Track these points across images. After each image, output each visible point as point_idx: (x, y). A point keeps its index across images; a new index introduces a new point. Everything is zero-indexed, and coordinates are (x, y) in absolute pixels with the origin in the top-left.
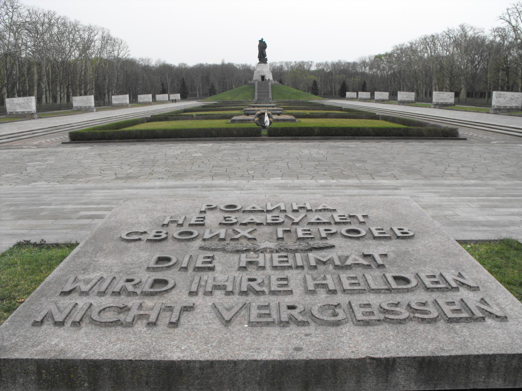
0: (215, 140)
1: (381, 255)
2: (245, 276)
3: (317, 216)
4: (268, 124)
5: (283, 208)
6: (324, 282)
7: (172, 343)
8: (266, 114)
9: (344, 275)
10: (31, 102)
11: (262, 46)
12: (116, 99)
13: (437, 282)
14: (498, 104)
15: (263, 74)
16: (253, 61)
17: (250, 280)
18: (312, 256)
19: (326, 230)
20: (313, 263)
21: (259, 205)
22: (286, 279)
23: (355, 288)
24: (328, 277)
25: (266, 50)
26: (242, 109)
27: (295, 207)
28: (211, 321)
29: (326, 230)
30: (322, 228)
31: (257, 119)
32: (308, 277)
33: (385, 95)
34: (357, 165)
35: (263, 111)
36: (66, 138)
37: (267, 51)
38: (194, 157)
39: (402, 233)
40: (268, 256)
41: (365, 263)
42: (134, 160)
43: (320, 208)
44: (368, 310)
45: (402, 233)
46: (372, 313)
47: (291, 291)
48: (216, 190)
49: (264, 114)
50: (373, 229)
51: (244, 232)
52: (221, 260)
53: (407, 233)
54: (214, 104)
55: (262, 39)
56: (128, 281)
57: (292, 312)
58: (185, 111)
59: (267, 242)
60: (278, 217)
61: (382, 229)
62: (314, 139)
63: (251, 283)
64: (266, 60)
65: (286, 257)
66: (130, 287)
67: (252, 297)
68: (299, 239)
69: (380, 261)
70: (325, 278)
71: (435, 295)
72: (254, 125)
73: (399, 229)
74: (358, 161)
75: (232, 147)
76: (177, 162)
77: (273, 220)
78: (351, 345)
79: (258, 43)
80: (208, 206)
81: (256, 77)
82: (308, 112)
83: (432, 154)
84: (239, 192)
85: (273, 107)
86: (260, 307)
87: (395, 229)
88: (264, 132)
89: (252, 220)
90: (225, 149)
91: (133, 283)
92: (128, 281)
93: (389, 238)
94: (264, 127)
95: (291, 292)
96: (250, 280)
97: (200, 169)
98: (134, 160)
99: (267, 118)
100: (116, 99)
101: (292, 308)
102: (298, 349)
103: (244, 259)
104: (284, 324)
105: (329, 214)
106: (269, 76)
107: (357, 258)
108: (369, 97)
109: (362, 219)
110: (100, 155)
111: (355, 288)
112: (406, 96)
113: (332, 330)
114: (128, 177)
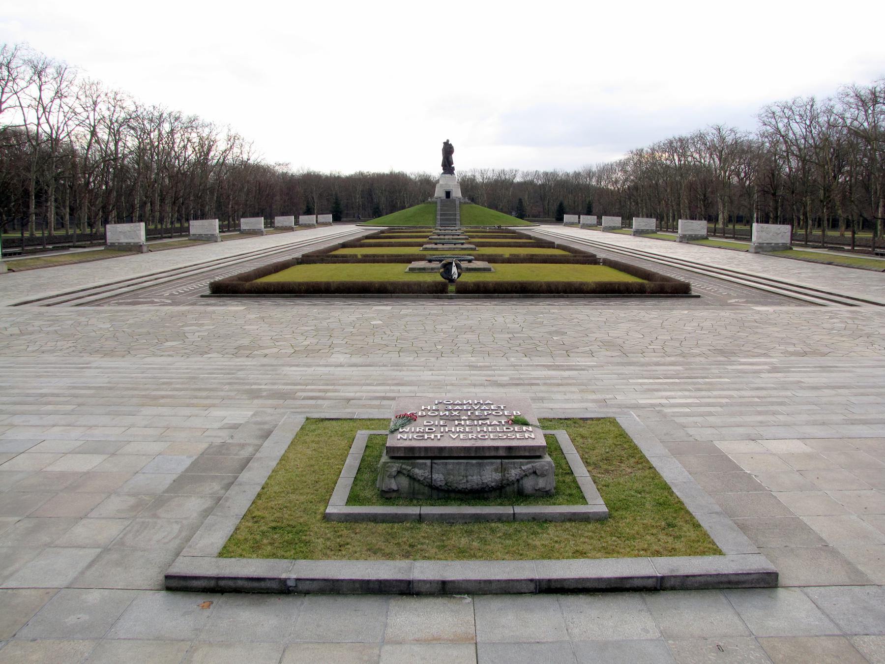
0: (392, 297)
4: (456, 276)
10: (140, 230)
11: (448, 150)
12: (246, 224)
14: (760, 241)
15: (448, 189)
16: (435, 170)
18: (480, 422)
25: (453, 156)
31: (442, 270)
33: (617, 221)
34: (555, 338)
35: (449, 260)
36: (208, 292)
37: (455, 157)
42: (306, 328)
48: (408, 370)
49: (451, 263)
51: (456, 413)
52: (448, 423)
54: (382, 232)
55: (448, 141)
58: (344, 246)
62: (512, 297)
64: (453, 169)
72: (439, 278)
74: (557, 333)
75: (415, 312)
76: (354, 331)
79: (442, 146)
81: (439, 193)
82: (507, 252)
83: (645, 322)
84: (430, 373)
85: (462, 244)
88: (452, 288)
90: (407, 315)
94: (452, 281)
97: (383, 343)
98: (306, 328)
99: (454, 270)
100: (246, 224)
103: (457, 422)
106: (457, 193)
108: (595, 222)
110: (263, 319)
114: (309, 351)
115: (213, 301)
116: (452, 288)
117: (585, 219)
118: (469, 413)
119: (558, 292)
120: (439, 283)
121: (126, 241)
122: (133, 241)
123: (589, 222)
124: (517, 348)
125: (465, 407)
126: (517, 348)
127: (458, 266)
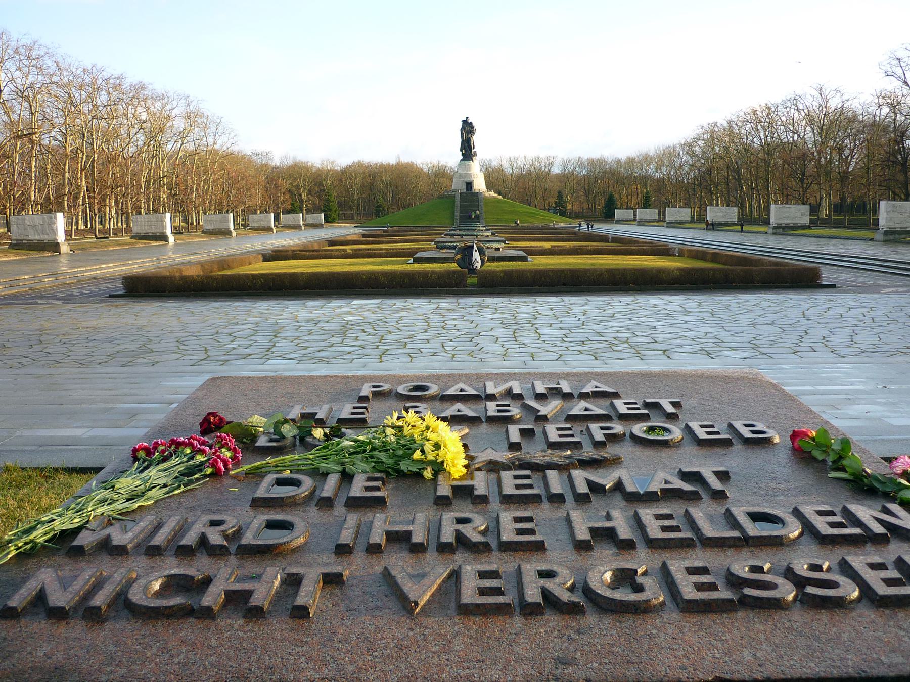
1: (717, 473)
2: (448, 517)
3: (583, 404)
4: (479, 265)
5: (517, 390)
6: (608, 524)
7: (298, 649)
8: (475, 248)
9: (648, 511)
11: (468, 129)
13: (840, 525)
14: (892, 224)
15: (468, 179)
17: (460, 521)
19: (602, 428)
20: (583, 488)
21: (470, 385)
22: (530, 520)
23: (673, 535)
24: (615, 514)
26: (432, 241)
27: (540, 388)
28: (379, 604)
29: (602, 428)
30: (594, 427)
31: (459, 256)
32: (577, 516)
33: (685, 214)
37: (476, 140)
38: (348, 321)
39: (753, 432)
40: (493, 476)
41: (687, 487)
43: (588, 389)
44: (704, 579)
45: (753, 432)
46: (712, 587)
47: (542, 543)
49: (472, 247)
50: (695, 426)
53: (764, 433)
56: (214, 524)
57: (549, 584)
58: (332, 243)
59: (489, 450)
60: (509, 405)
61: (712, 426)
63: (460, 527)
64: (475, 154)
65: (527, 477)
66: (215, 537)
67: (460, 557)
68: (552, 445)
69: (716, 484)
70: (608, 517)
71: (840, 552)
72: (454, 266)
73: (746, 426)
77: (499, 411)
78: (679, 654)
80: (374, 387)
82: (547, 245)
86: (483, 575)
87: (738, 425)
89: (461, 390)
91: (222, 528)
92: (214, 524)
93: (727, 443)
94: (472, 271)
95: (539, 547)
96: (460, 521)
99: (476, 255)
101: (548, 575)
102: (562, 662)
104: (530, 611)
105: (606, 402)
107: (669, 478)
109: (670, 409)
111: (673, 535)
112: (721, 214)
113: (630, 621)
115: (122, 302)
116: (472, 280)
117: (642, 214)
118: (514, 433)
119: (626, 284)
120: (454, 272)
121: (37, 237)
122: (46, 237)
123: (648, 217)
124: (579, 348)
125: (492, 408)
126: (579, 348)
127: (481, 251)
